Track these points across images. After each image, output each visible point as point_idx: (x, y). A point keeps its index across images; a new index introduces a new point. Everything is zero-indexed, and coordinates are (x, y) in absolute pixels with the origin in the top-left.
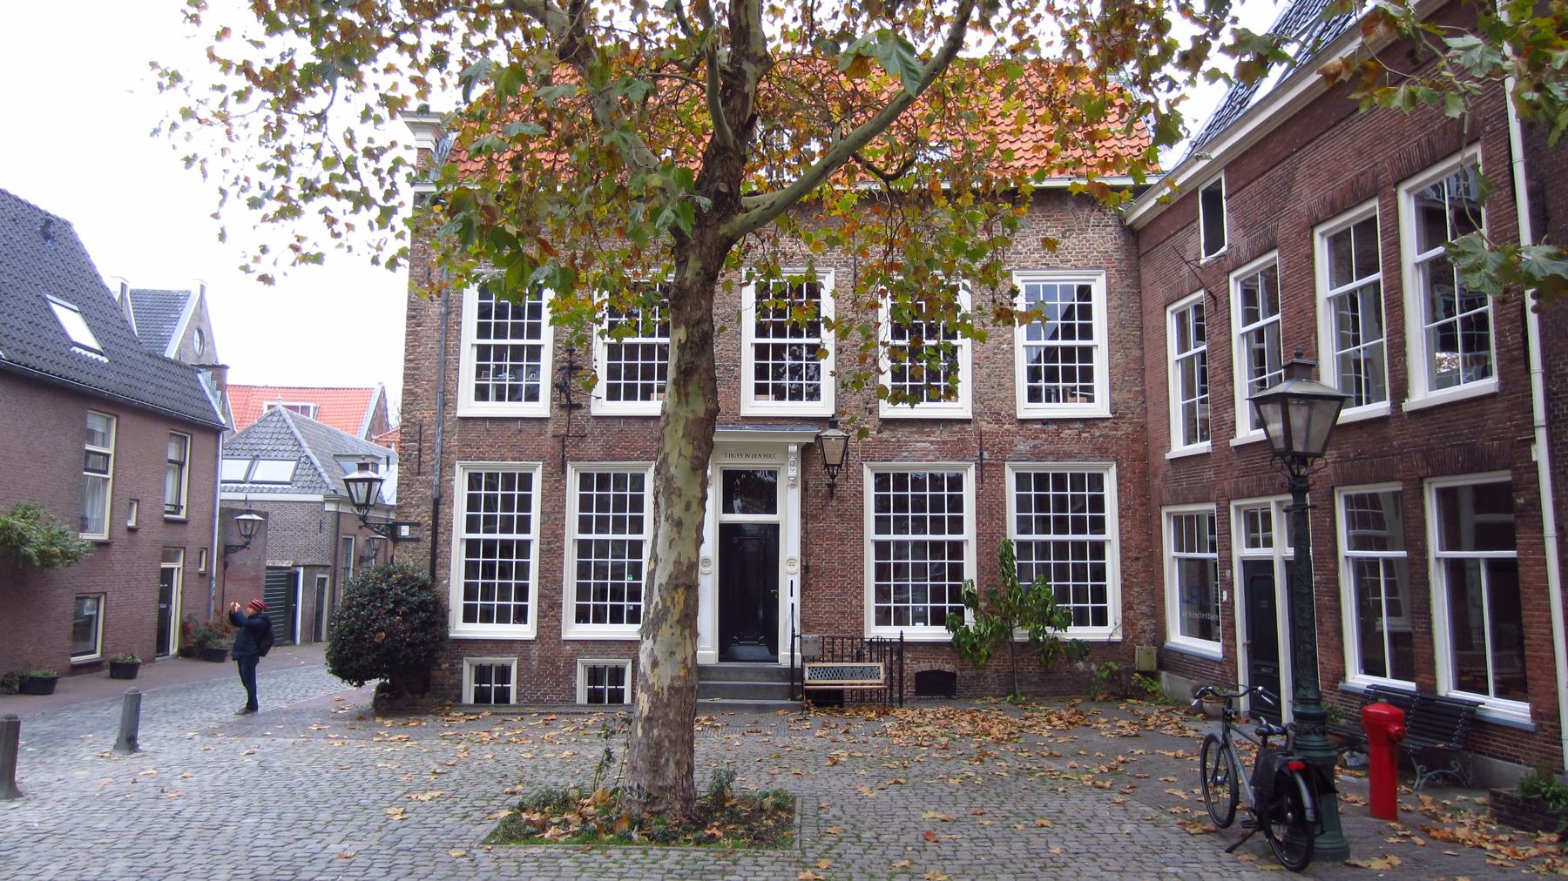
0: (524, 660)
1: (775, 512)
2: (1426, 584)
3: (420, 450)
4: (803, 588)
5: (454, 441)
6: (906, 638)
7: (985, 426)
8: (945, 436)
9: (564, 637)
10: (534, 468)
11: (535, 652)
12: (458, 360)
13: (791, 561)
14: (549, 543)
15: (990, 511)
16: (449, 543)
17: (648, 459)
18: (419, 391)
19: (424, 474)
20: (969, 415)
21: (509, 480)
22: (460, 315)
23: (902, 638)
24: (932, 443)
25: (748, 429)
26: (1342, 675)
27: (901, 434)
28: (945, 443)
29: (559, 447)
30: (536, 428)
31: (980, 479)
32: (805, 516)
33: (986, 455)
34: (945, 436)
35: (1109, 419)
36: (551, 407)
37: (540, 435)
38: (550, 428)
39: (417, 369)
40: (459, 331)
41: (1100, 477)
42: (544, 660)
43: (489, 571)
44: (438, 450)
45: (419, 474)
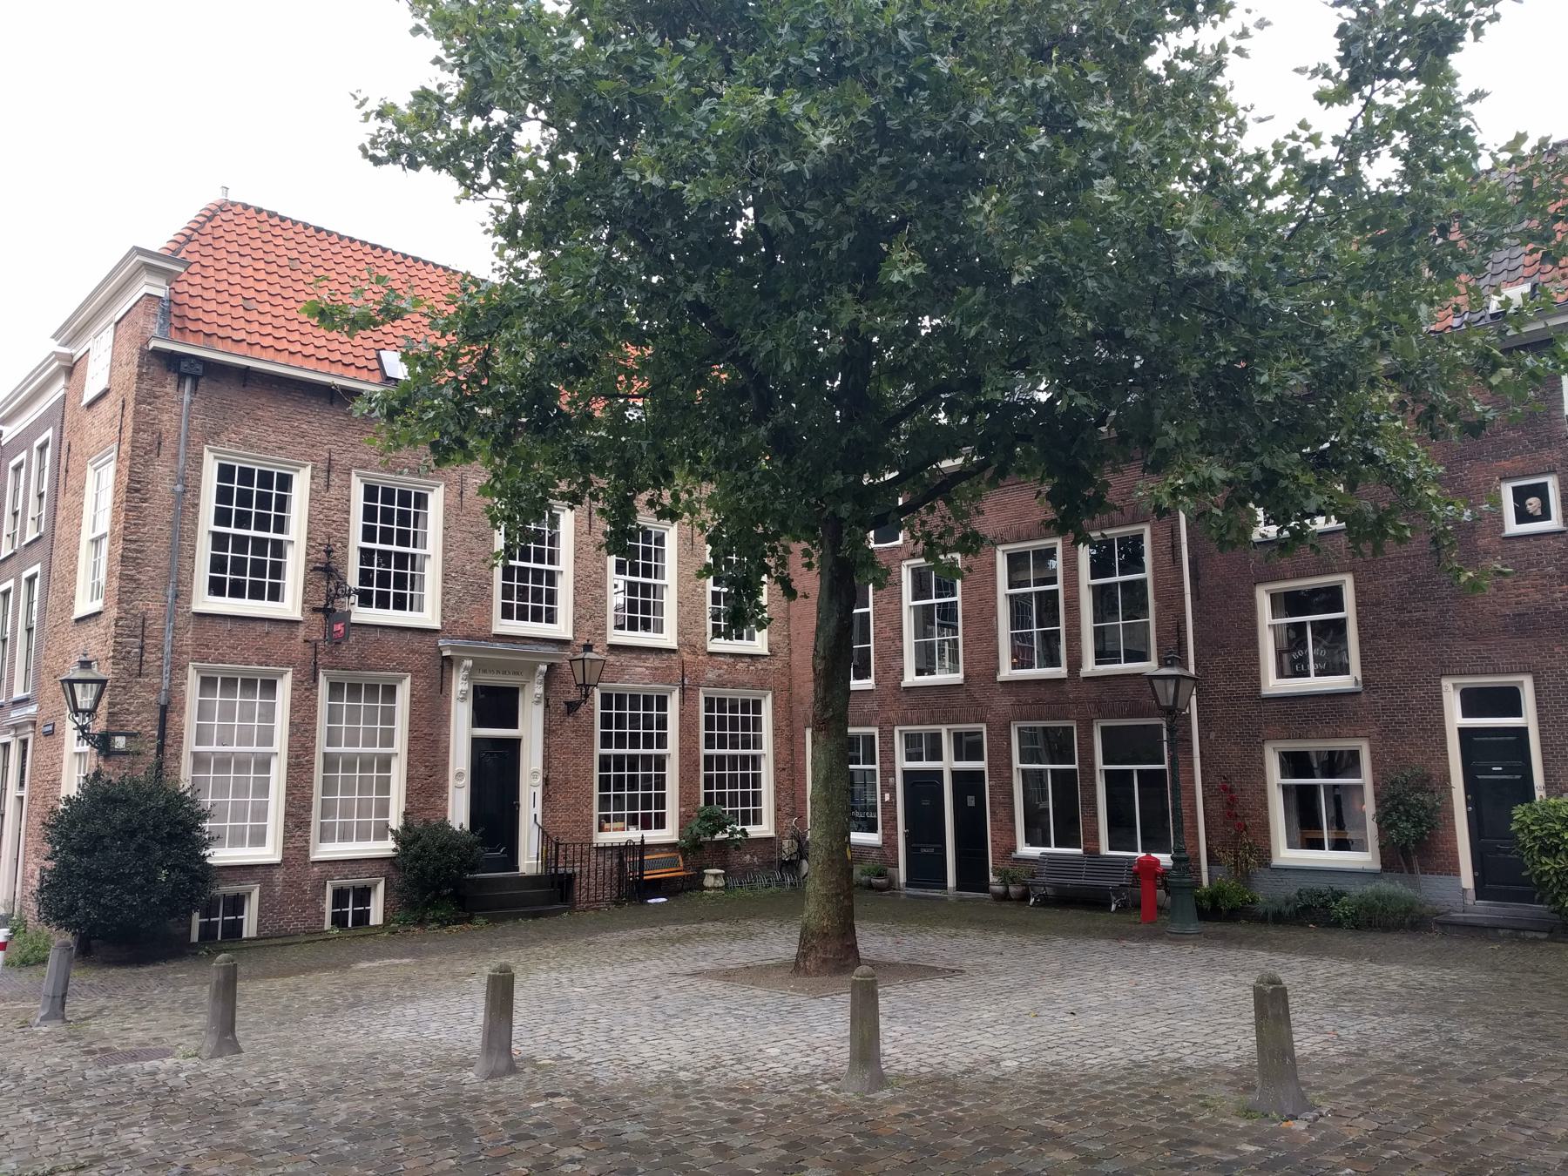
0: (267, 886)
1: (516, 727)
2: (1093, 785)
3: (142, 648)
4: (544, 799)
5: (188, 638)
6: (647, 841)
7: (687, 657)
8: (657, 663)
9: (314, 857)
10: (281, 675)
11: (279, 876)
12: (193, 548)
13: (459, 775)
14: (298, 757)
15: (687, 729)
16: (178, 756)
17: (403, 671)
18: (143, 578)
19: (147, 675)
20: (674, 645)
21: (745, 705)
22: (198, 497)
23: (643, 841)
24: (647, 668)
25: (499, 646)
26: (1014, 849)
27: (624, 658)
28: (656, 669)
29: (311, 652)
30: (282, 633)
31: (682, 701)
32: (548, 732)
33: (686, 681)
34: (657, 663)
35: (764, 656)
36: (303, 609)
37: (289, 639)
38: (301, 632)
39: (141, 552)
40: (196, 515)
41: (665, 698)
42: (289, 884)
43: (619, 783)
44: (168, 649)
45: (140, 675)
